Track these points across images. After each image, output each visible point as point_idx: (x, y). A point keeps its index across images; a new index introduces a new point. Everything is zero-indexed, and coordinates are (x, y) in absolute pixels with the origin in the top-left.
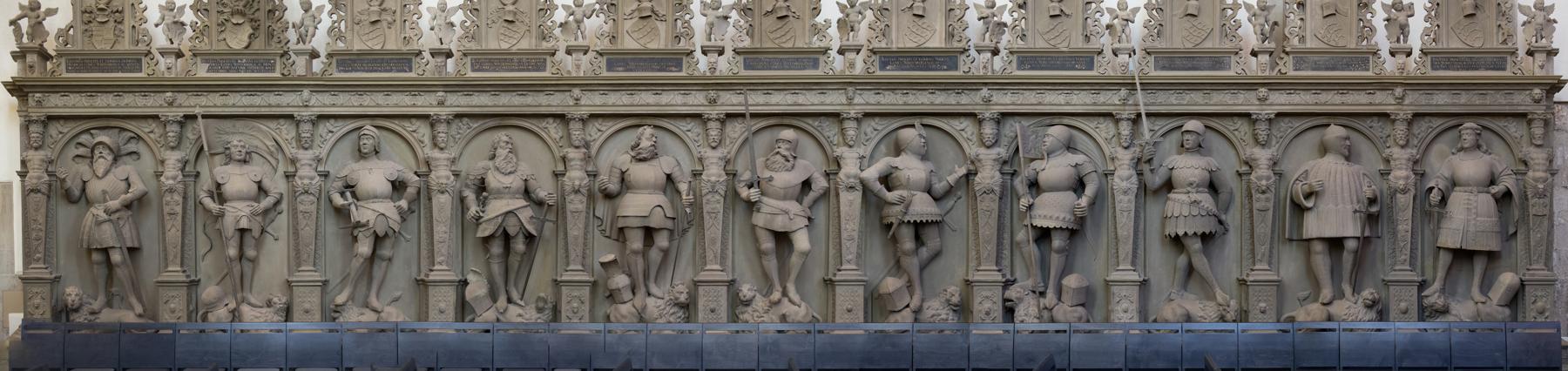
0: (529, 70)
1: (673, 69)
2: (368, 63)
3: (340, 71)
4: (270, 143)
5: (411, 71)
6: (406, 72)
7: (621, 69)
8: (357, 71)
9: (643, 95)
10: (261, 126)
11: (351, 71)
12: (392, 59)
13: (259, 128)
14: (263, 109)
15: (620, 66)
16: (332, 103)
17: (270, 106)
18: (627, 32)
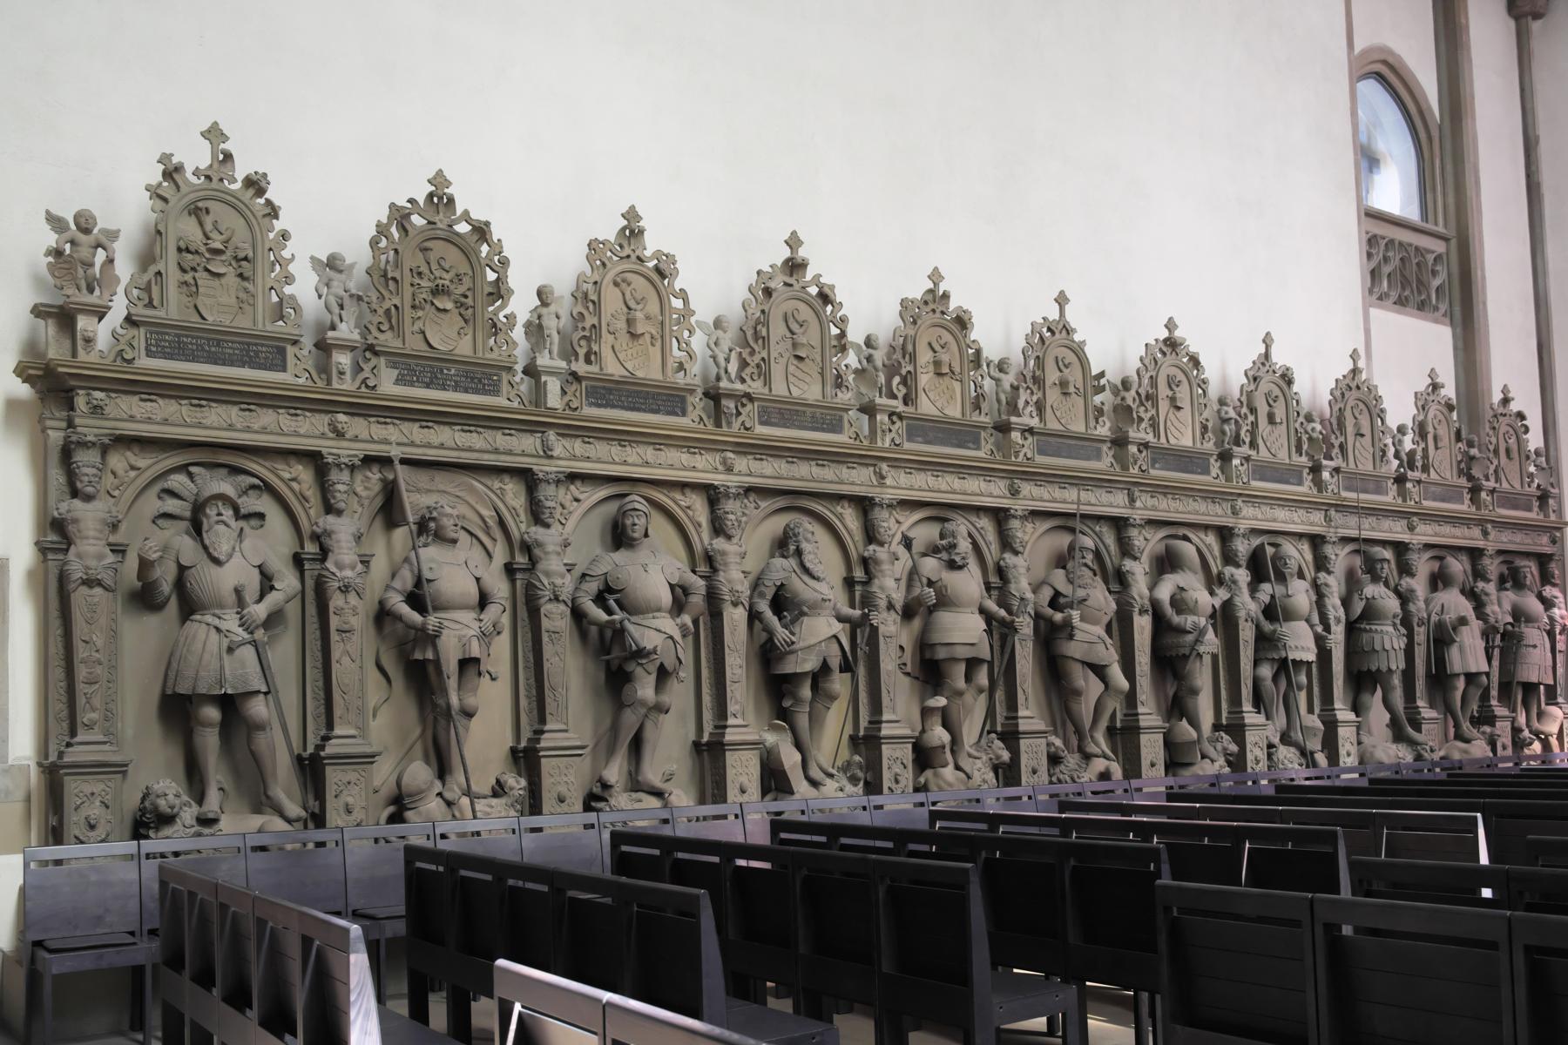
0: (823, 430)
1: (971, 445)
2: (628, 396)
3: (591, 404)
4: (487, 513)
5: (684, 414)
6: (677, 415)
7: (920, 439)
8: (613, 407)
9: (949, 478)
10: (476, 484)
11: (605, 406)
12: (659, 394)
13: (472, 485)
14: (486, 456)
15: (919, 436)
16: (587, 455)
17: (496, 451)
18: (924, 390)
